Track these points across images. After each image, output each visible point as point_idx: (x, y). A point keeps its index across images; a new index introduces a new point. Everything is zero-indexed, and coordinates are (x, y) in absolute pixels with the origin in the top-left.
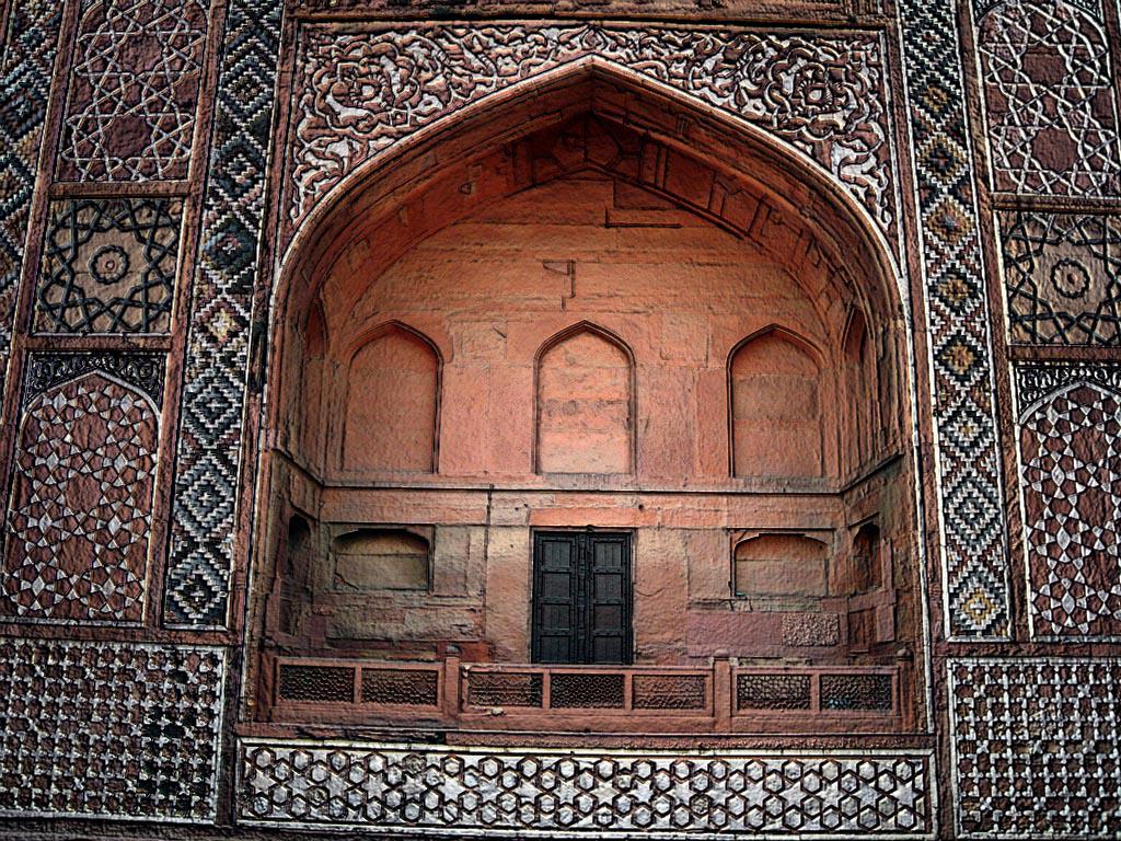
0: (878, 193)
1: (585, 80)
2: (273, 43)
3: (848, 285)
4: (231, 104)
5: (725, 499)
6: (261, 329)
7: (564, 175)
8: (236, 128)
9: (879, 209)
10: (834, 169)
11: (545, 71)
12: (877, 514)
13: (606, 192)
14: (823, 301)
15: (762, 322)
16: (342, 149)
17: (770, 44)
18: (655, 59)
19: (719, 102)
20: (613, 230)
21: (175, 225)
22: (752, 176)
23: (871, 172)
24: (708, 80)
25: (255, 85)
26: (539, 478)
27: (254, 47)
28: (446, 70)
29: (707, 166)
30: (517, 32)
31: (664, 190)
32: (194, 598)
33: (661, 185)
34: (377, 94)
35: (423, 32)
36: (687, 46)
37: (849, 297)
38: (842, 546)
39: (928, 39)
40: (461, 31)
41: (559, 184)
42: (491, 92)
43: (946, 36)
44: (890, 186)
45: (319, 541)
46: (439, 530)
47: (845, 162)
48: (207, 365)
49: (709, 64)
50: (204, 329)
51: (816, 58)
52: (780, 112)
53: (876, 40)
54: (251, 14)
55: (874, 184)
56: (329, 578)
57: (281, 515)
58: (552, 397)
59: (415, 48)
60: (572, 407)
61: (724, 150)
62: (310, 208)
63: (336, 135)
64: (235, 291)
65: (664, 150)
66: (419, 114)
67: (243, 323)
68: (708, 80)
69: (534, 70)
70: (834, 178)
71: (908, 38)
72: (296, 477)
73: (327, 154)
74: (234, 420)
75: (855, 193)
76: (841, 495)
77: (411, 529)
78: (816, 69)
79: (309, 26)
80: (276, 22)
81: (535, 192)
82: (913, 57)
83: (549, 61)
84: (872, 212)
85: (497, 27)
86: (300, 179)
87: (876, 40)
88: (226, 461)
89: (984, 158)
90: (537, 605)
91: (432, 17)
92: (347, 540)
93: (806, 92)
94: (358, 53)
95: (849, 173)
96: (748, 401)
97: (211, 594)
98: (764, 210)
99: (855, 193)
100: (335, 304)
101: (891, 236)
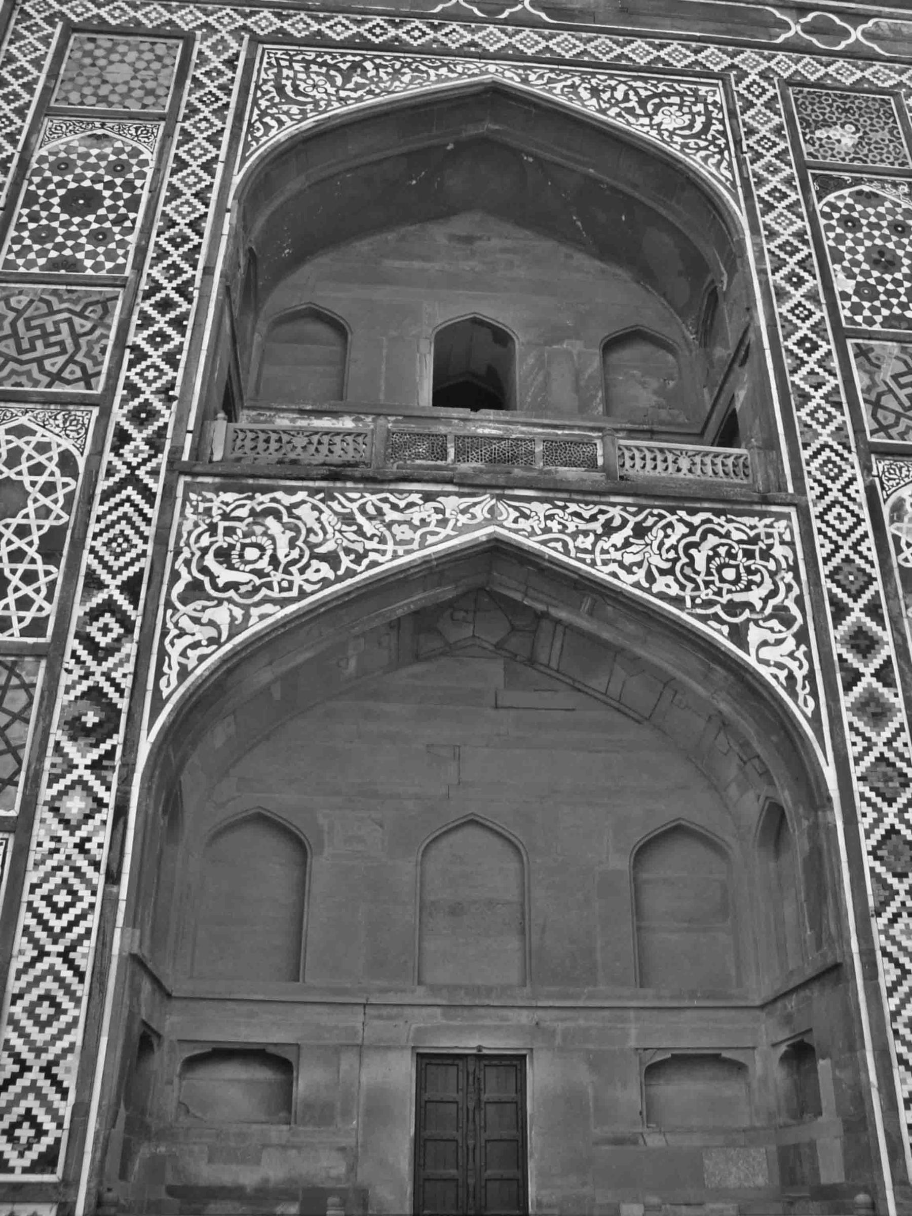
0: (799, 675)
1: (485, 551)
2: (149, 497)
3: (765, 773)
4: (101, 559)
5: (632, 1014)
6: (121, 811)
7: (449, 650)
8: (102, 586)
9: (801, 694)
10: (752, 650)
11: (443, 542)
12: (810, 1031)
13: (495, 670)
14: (733, 791)
15: (667, 811)
16: (221, 615)
17: (681, 520)
18: (560, 532)
19: (631, 579)
20: (502, 711)
21: (28, 688)
22: (659, 655)
23: (791, 655)
24: (617, 555)
25: (127, 539)
26: (421, 990)
27: (128, 499)
28: (338, 535)
29: (606, 645)
30: (415, 498)
31: (558, 671)
32: (18, 1138)
33: (554, 665)
34: (261, 557)
35: (313, 492)
36: (593, 518)
37: (765, 790)
38: (767, 1068)
39: (839, 518)
40: (352, 495)
41: (443, 660)
42: (388, 560)
43: (857, 516)
44: (812, 670)
45: (164, 1062)
46: (303, 1052)
47: (765, 643)
48: (57, 851)
49: (618, 539)
50: (55, 810)
51: (728, 535)
52: (693, 590)
53: (787, 517)
54: (128, 464)
55: (794, 665)
56: (171, 1107)
57: (129, 1029)
58: (432, 898)
59: (304, 511)
60: (456, 910)
61: (631, 628)
62: (184, 673)
63: (213, 599)
64: (95, 766)
65: (560, 629)
66: (307, 581)
67: (100, 804)
68: (617, 555)
69: (431, 539)
70: (751, 660)
71: (820, 517)
72: (147, 986)
73: (204, 621)
74: (82, 916)
75: (776, 677)
76: (762, 1007)
77: (271, 1050)
78: (731, 547)
79: (188, 479)
80: (154, 473)
81: (418, 668)
82: (825, 535)
83: (448, 531)
84: (794, 695)
85: (392, 492)
86: (172, 644)
87: (787, 517)
88: (71, 965)
89: (905, 640)
90: (421, 1145)
91: (324, 478)
92: (192, 1063)
93: (720, 569)
94: (243, 512)
95: (771, 654)
96: (658, 901)
97: (41, 1132)
98: (668, 694)
99: (776, 677)
100: (192, 783)
101: (815, 720)
